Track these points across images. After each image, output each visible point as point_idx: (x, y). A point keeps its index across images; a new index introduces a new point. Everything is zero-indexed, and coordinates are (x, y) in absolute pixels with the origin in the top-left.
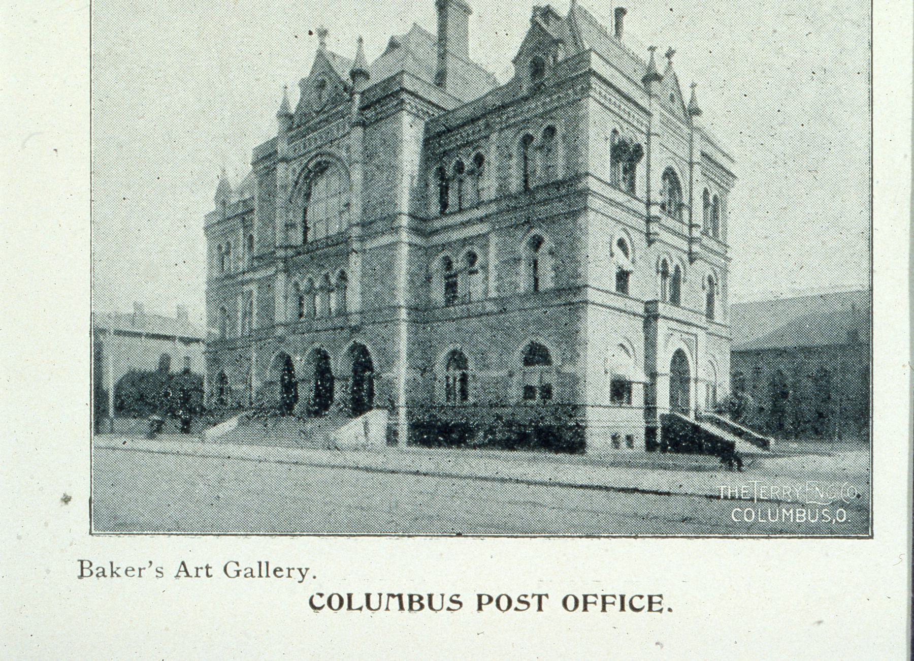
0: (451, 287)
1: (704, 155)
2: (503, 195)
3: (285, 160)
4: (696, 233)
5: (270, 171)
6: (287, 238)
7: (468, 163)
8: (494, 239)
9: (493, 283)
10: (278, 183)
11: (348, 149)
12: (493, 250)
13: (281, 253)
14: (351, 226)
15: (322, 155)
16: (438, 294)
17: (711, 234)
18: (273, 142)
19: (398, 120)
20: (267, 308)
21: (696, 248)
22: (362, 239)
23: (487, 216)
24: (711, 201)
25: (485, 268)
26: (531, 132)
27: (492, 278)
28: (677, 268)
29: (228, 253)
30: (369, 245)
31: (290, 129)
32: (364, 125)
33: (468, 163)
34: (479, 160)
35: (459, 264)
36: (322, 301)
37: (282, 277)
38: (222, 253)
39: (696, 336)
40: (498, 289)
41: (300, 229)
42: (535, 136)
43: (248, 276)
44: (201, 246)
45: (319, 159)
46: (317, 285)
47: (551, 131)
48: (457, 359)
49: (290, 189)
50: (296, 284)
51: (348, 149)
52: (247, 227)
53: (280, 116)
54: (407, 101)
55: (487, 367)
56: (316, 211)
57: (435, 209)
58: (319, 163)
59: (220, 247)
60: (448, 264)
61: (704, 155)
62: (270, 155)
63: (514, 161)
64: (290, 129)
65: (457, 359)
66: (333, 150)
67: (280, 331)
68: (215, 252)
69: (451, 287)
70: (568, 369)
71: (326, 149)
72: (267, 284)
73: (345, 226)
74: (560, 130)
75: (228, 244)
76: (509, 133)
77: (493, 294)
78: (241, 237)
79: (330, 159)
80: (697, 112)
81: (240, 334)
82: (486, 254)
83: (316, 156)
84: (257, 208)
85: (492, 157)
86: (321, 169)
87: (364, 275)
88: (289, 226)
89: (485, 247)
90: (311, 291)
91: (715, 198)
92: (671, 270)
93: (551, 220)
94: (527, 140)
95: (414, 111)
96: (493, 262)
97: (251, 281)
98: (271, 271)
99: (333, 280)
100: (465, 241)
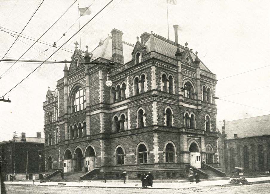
0: (118, 126)
1: (201, 75)
2: (131, 97)
3: (67, 85)
4: (200, 102)
5: (63, 88)
6: (68, 112)
7: (121, 86)
8: (129, 111)
9: (129, 125)
10: (65, 93)
11: (85, 82)
12: (129, 114)
13: (66, 116)
14: (87, 107)
15: (77, 84)
16: (114, 128)
17: (207, 102)
18: (63, 79)
19: (98, 73)
20: (62, 134)
21: (200, 108)
22: (90, 111)
23: (127, 103)
24: (207, 90)
25: (127, 119)
26: (138, 76)
27: (129, 123)
28: (192, 115)
29: (51, 115)
30: (92, 113)
31: (68, 75)
32: (89, 75)
33: (121, 86)
34: (124, 85)
35: (119, 119)
36: (79, 131)
37: (66, 124)
38: (48, 115)
40: (131, 127)
41: (72, 109)
42: (139, 78)
43: (57, 123)
44: (43, 113)
46: (77, 127)
47: (143, 77)
48: (120, 150)
49: (68, 95)
50: (71, 126)
51: (85, 82)
52: (56, 106)
53: (64, 71)
55: (129, 152)
56: (77, 102)
57: (112, 101)
58: (76, 87)
59: (48, 113)
60: (116, 118)
61: (201, 75)
62: (62, 83)
63: (134, 86)
64: (68, 75)
65: (120, 150)
66: (81, 82)
67: (66, 143)
68: (47, 115)
69: (118, 126)
70: (151, 152)
71: (78, 82)
72: (62, 126)
73: (85, 107)
74: (146, 76)
75: (51, 112)
76: (132, 76)
77: (129, 128)
78: (55, 110)
79: (80, 86)
81: (55, 144)
82: (127, 115)
83: (75, 84)
84: (59, 101)
85: (127, 83)
86: (76, 89)
87: (90, 124)
88: (69, 107)
89: (127, 114)
90: (76, 129)
91: (209, 89)
92: (190, 116)
93: (145, 105)
94: (137, 79)
95: (104, 70)
96: (129, 118)
97: (58, 125)
98: (63, 122)
99: (82, 125)
100: (122, 111)
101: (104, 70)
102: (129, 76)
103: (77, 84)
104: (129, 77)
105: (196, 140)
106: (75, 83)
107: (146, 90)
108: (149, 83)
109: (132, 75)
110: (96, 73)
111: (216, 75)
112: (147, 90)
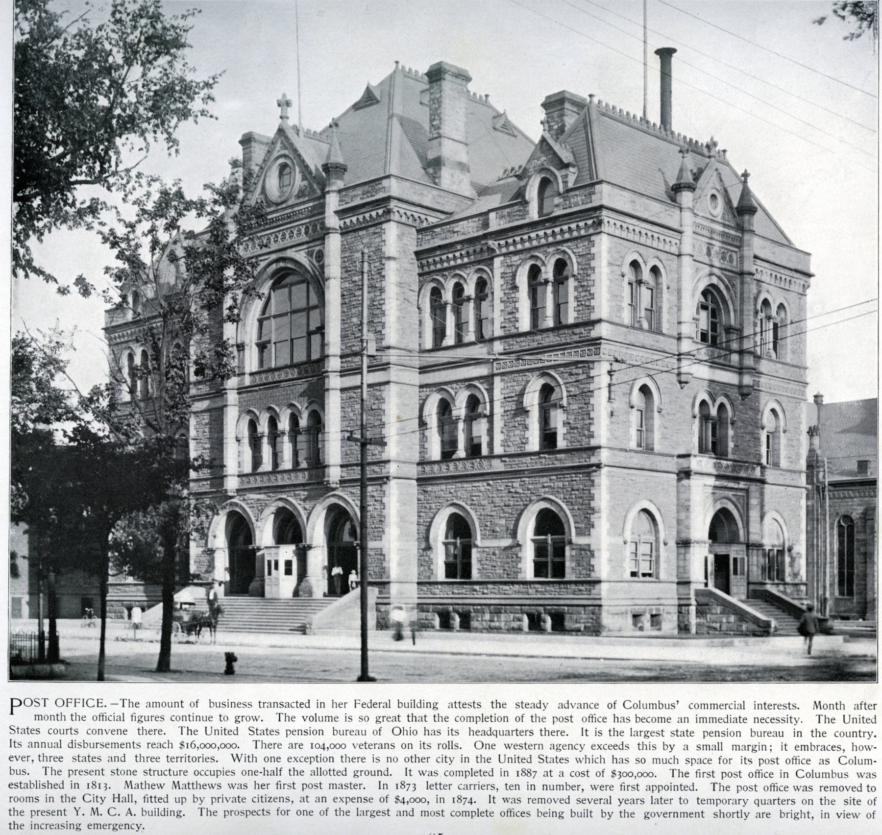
28: (722, 406)
39: (747, 491)
45: (282, 264)
54: (395, 209)
71: (290, 253)
80: (752, 211)
83: (277, 261)
85: (497, 285)
101: (404, 219)
102: (504, 255)
103: (283, 259)
104: (502, 258)
105: (734, 499)
106: (274, 257)
107: (571, 317)
108: (583, 294)
109: (515, 253)
110: (371, 230)
111: (809, 254)
112: (575, 318)
